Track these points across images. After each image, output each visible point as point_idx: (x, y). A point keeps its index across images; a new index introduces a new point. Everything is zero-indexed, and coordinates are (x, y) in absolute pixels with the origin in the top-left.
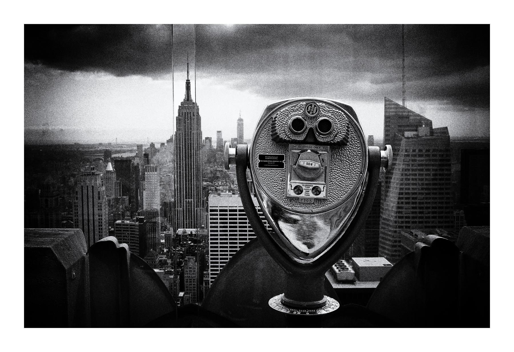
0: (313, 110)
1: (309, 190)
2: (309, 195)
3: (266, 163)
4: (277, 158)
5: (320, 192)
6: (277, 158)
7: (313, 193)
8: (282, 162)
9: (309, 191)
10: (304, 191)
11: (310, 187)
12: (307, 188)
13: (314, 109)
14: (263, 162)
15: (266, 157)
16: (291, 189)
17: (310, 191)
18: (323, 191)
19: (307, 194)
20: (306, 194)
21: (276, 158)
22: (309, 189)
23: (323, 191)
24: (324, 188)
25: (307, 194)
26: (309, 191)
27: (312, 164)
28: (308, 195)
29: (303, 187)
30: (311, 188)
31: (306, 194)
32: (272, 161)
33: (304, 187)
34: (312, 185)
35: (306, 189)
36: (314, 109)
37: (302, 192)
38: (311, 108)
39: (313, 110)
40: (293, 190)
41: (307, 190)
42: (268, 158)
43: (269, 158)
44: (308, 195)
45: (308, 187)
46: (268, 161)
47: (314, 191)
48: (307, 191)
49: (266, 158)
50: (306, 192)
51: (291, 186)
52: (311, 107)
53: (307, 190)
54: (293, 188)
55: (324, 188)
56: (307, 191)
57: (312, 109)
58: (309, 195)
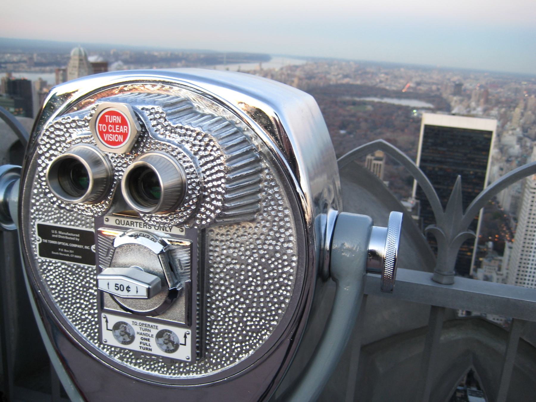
0: (112, 133)
1: (148, 337)
2: (151, 350)
3: (56, 248)
4: (78, 237)
5: (176, 347)
6: (78, 237)
7: (160, 345)
8: (90, 248)
9: (148, 340)
10: (138, 338)
11: (152, 330)
12: (143, 332)
13: (115, 133)
14: (48, 244)
15: (53, 232)
16: (108, 329)
17: (153, 342)
18: (185, 345)
19: (146, 346)
20: (142, 345)
21: (75, 237)
22: (150, 334)
23: (185, 345)
24: (185, 337)
25: (146, 346)
26: (148, 340)
27: (128, 287)
28: (147, 349)
29: (134, 327)
30: (154, 332)
31: (142, 345)
32: (67, 244)
33: (136, 329)
34: (157, 327)
35: (141, 334)
36: (115, 133)
37: (132, 338)
39: (112, 133)
40: (111, 332)
41: (144, 337)
42: (58, 234)
43: (60, 237)
44: (147, 349)
45: (146, 330)
46: (60, 243)
47: (161, 340)
48: (145, 339)
49: (54, 234)
50: (144, 341)
51: (107, 321)
52: (118, 124)
53: (146, 337)
54: (111, 327)
55: (185, 337)
56: (145, 339)
57: (115, 129)
58: (151, 350)
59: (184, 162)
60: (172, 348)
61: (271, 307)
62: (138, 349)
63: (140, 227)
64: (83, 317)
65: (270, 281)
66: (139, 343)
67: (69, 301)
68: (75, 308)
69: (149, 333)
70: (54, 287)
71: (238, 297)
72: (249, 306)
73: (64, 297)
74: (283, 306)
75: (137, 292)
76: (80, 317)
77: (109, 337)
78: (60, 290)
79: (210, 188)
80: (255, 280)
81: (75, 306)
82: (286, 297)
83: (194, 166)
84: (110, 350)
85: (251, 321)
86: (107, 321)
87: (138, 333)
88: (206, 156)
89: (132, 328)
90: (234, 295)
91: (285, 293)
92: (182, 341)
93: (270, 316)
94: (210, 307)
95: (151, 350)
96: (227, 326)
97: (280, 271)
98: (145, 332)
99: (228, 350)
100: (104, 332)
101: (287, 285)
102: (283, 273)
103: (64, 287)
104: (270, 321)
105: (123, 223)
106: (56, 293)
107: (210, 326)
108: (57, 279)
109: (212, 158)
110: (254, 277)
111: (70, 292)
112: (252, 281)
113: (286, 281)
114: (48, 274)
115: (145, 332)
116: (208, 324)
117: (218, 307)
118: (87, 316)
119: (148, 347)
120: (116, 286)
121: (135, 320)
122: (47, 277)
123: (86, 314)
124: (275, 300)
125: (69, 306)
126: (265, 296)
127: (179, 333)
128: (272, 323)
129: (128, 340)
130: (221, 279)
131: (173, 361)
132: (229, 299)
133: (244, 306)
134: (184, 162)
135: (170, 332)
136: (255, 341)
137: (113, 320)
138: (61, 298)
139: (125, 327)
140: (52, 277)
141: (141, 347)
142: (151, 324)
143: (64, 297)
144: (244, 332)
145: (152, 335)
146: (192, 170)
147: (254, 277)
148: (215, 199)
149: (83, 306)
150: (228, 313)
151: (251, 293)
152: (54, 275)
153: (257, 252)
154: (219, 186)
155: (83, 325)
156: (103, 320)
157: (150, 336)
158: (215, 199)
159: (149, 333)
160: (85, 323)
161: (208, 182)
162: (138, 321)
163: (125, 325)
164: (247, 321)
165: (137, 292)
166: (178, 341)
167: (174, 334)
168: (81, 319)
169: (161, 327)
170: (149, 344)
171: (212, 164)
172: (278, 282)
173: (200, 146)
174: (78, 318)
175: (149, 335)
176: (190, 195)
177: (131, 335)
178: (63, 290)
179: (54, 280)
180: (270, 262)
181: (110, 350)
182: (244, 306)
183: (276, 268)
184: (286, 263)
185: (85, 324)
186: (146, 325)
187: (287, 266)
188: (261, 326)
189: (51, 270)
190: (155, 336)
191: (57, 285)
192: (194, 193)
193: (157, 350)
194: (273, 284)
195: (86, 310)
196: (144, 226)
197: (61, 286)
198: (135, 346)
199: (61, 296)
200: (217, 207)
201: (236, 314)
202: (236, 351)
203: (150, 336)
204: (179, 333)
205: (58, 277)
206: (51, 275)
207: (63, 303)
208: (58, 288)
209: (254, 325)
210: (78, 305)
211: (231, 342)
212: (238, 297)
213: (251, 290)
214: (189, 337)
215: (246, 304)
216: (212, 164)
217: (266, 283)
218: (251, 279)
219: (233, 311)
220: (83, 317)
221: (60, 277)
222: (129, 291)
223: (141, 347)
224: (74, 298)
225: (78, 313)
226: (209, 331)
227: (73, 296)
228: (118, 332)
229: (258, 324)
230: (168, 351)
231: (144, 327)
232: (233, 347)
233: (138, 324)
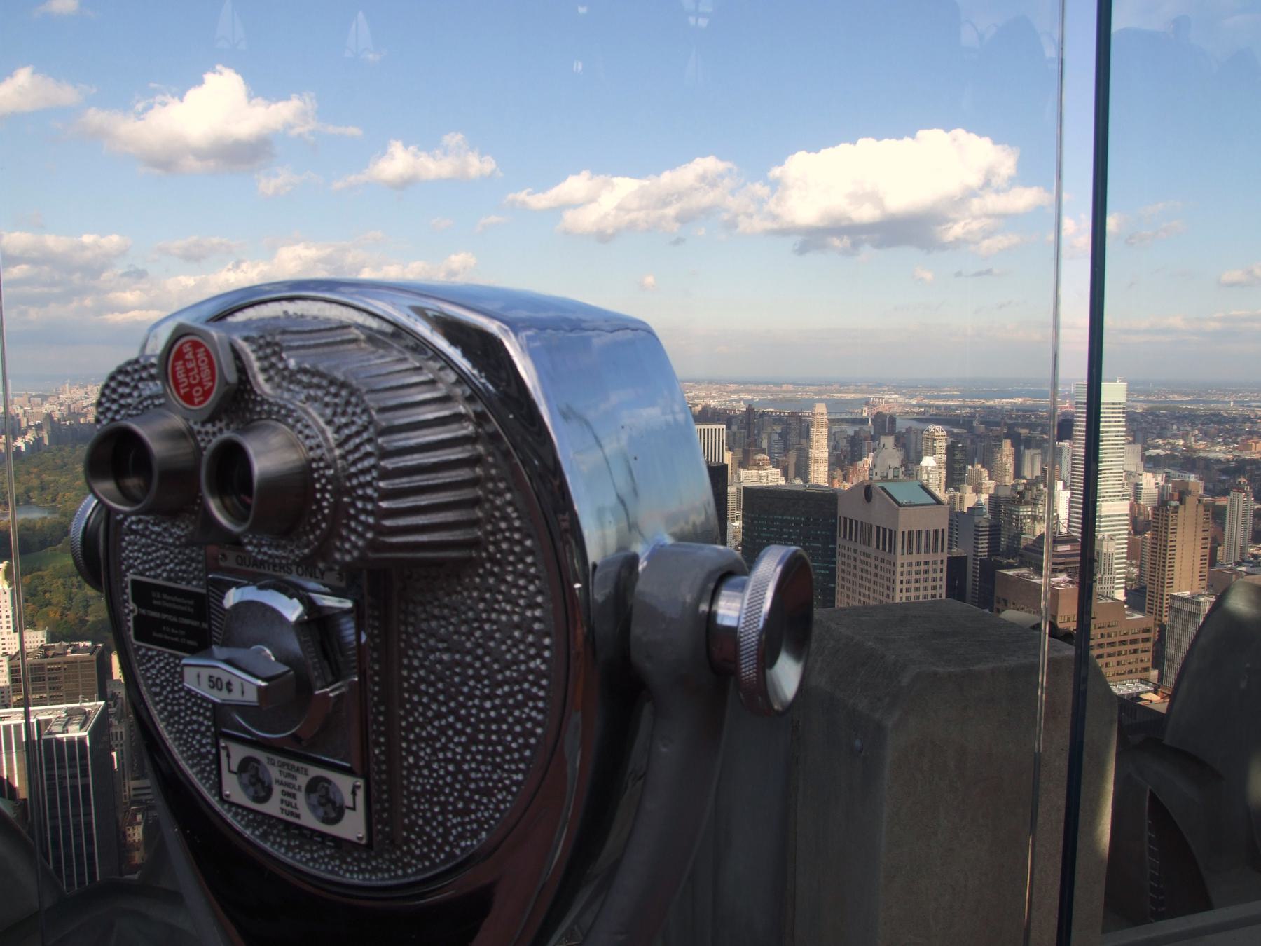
1: (293, 791)
7: (313, 808)
9: (294, 796)
10: (277, 790)
12: (285, 780)
17: (301, 799)
18: (354, 809)
19: (289, 809)
22: (297, 783)
23: (354, 809)
25: (289, 809)
26: (294, 796)
28: (292, 814)
29: (269, 767)
30: (302, 781)
31: (284, 806)
33: (274, 773)
38: (188, 371)
41: (287, 789)
44: (292, 814)
45: (288, 775)
48: (289, 795)
50: (286, 798)
51: (228, 756)
54: (234, 767)
55: (354, 793)
56: (289, 795)
59: (307, 437)
60: (333, 815)
61: (511, 742)
62: (277, 813)
63: (274, 570)
64: (203, 750)
65: (506, 688)
66: (280, 802)
67: (181, 718)
68: (190, 731)
69: (293, 782)
70: (158, 690)
71: (451, 719)
72: (473, 740)
73: (173, 709)
74: (533, 741)
75: (243, 693)
76: (198, 750)
77: (233, 788)
78: (166, 697)
79: (354, 488)
80: (479, 686)
81: (190, 728)
82: (537, 723)
83: (324, 444)
84: (246, 819)
85: (477, 770)
86: (228, 756)
87: (277, 781)
88: (346, 425)
89: (266, 770)
90: (445, 716)
91: (534, 714)
92: (348, 801)
93: (509, 762)
94: (406, 739)
95: (298, 816)
96: (436, 779)
97: (523, 667)
98: (289, 780)
99: (441, 830)
100: (227, 776)
101: (536, 698)
102: (530, 671)
103: (173, 691)
104: (510, 771)
105: (247, 563)
106: (161, 701)
107: (408, 778)
108: (163, 674)
109: (354, 429)
110: (478, 678)
111: (182, 701)
112: (475, 688)
113: (535, 690)
114: (149, 665)
115: (289, 780)
116: (405, 773)
117: (419, 738)
118: (209, 748)
119: (294, 810)
120: (210, 681)
121: (271, 756)
122: (147, 670)
123: (208, 744)
124: (518, 729)
125: (181, 727)
126: (500, 719)
127: (344, 784)
128: (515, 777)
129: (333, 815)
130: (421, 680)
131: (338, 842)
132: (436, 723)
133: (463, 739)
134: (307, 437)
135: (328, 781)
136: (486, 814)
137: (238, 753)
138: (169, 712)
139: (257, 768)
140: (154, 671)
141: (282, 809)
142: (297, 764)
143: (173, 709)
144: (467, 794)
145: (300, 787)
146: (319, 452)
147: (478, 678)
148: (364, 511)
149: (203, 729)
150: (435, 752)
151: (474, 711)
152: (157, 666)
153: (481, 628)
154: (369, 484)
155: (203, 766)
156: (223, 754)
157: (297, 787)
158: (364, 511)
159: (293, 782)
160: (207, 761)
161: (355, 475)
162: (277, 758)
163: (326, 785)
164: (472, 770)
165: (243, 693)
166: (342, 799)
167: (335, 785)
168: (200, 754)
169: (315, 771)
170: (296, 804)
171: (357, 441)
172: (521, 691)
173: (336, 405)
174: (195, 752)
175: (293, 787)
176: (318, 502)
177: (338, 805)
178: (171, 696)
179: (157, 677)
180: (504, 648)
181: (246, 819)
182: (463, 739)
183: (516, 661)
184: (532, 651)
185: (206, 765)
186: (288, 765)
187: (533, 658)
188: (495, 782)
189: (151, 658)
190: (303, 789)
191: (163, 688)
192: (324, 499)
193: (309, 819)
194: (512, 694)
195: (208, 737)
196: (280, 568)
197: (168, 689)
198: (272, 807)
199: (169, 708)
200: (368, 527)
201: (449, 755)
202: (454, 832)
203: (297, 787)
204: (344, 784)
205: (163, 671)
206: (153, 667)
207: (172, 721)
208: (165, 693)
209: (483, 779)
210: (195, 727)
211: (443, 812)
212: (451, 719)
213: (474, 706)
214: (361, 794)
215: (466, 734)
216: (357, 441)
217: (499, 692)
218: (472, 683)
219: (444, 748)
220: (203, 750)
221: (167, 671)
222: (230, 691)
223: (282, 809)
224: (189, 712)
225: (194, 743)
226: (407, 788)
227: (188, 708)
228: (246, 776)
229: (490, 779)
230: (327, 820)
231: (285, 770)
232: (449, 824)
233: (276, 764)
